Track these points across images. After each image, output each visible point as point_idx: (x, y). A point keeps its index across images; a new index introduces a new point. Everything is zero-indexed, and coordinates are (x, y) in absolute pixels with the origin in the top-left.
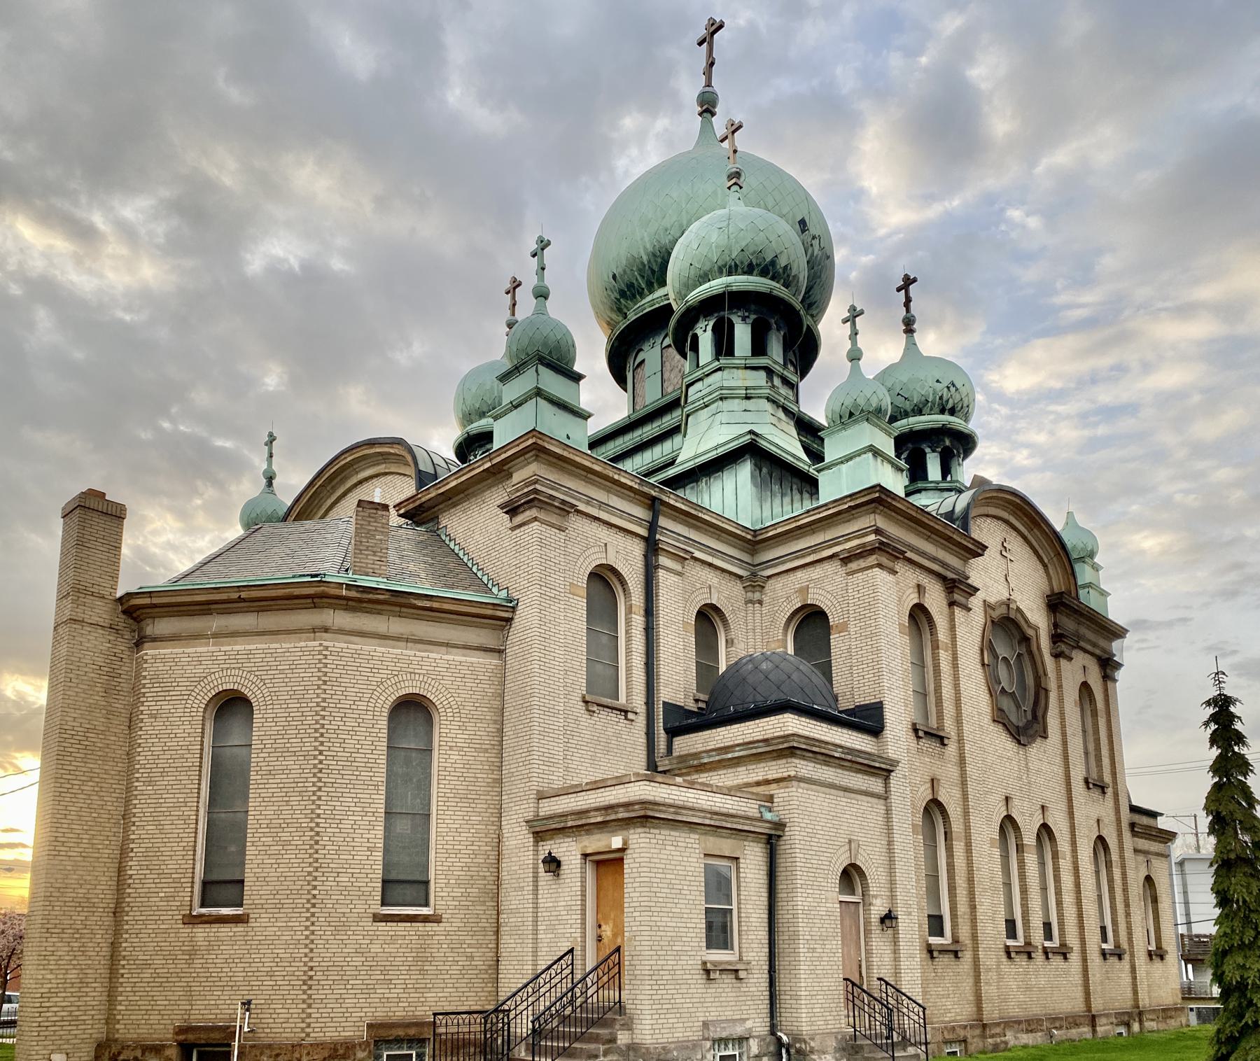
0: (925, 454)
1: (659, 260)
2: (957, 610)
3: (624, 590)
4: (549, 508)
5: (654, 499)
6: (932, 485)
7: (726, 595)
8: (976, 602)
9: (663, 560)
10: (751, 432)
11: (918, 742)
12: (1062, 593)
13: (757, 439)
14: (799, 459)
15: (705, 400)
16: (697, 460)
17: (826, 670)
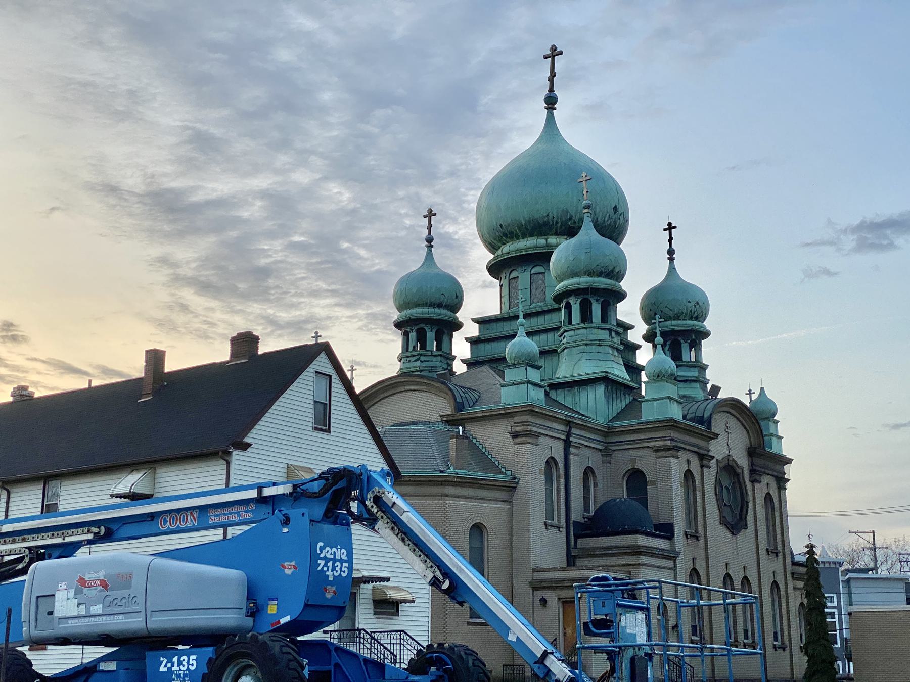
0: (680, 344)
1: (532, 225)
2: (705, 470)
3: (556, 467)
4: (533, 436)
5: (569, 422)
6: (685, 363)
7: (594, 460)
8: (713, 463)
9: (572, 450)
10: (605, 372)
11: (687, 540)
12: (756, 448)
13: (608, 375)
14: (625, 379)
15: (576, 343)
16: (573, 378)
17: (644, 502)
